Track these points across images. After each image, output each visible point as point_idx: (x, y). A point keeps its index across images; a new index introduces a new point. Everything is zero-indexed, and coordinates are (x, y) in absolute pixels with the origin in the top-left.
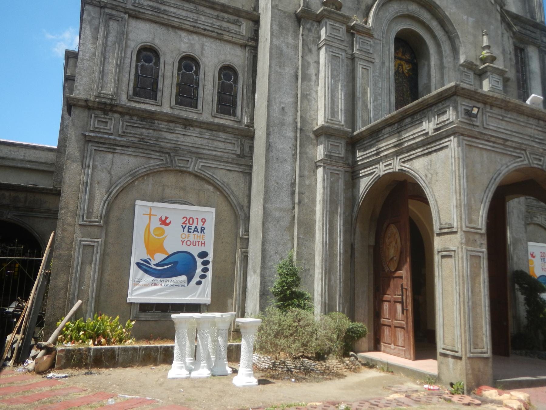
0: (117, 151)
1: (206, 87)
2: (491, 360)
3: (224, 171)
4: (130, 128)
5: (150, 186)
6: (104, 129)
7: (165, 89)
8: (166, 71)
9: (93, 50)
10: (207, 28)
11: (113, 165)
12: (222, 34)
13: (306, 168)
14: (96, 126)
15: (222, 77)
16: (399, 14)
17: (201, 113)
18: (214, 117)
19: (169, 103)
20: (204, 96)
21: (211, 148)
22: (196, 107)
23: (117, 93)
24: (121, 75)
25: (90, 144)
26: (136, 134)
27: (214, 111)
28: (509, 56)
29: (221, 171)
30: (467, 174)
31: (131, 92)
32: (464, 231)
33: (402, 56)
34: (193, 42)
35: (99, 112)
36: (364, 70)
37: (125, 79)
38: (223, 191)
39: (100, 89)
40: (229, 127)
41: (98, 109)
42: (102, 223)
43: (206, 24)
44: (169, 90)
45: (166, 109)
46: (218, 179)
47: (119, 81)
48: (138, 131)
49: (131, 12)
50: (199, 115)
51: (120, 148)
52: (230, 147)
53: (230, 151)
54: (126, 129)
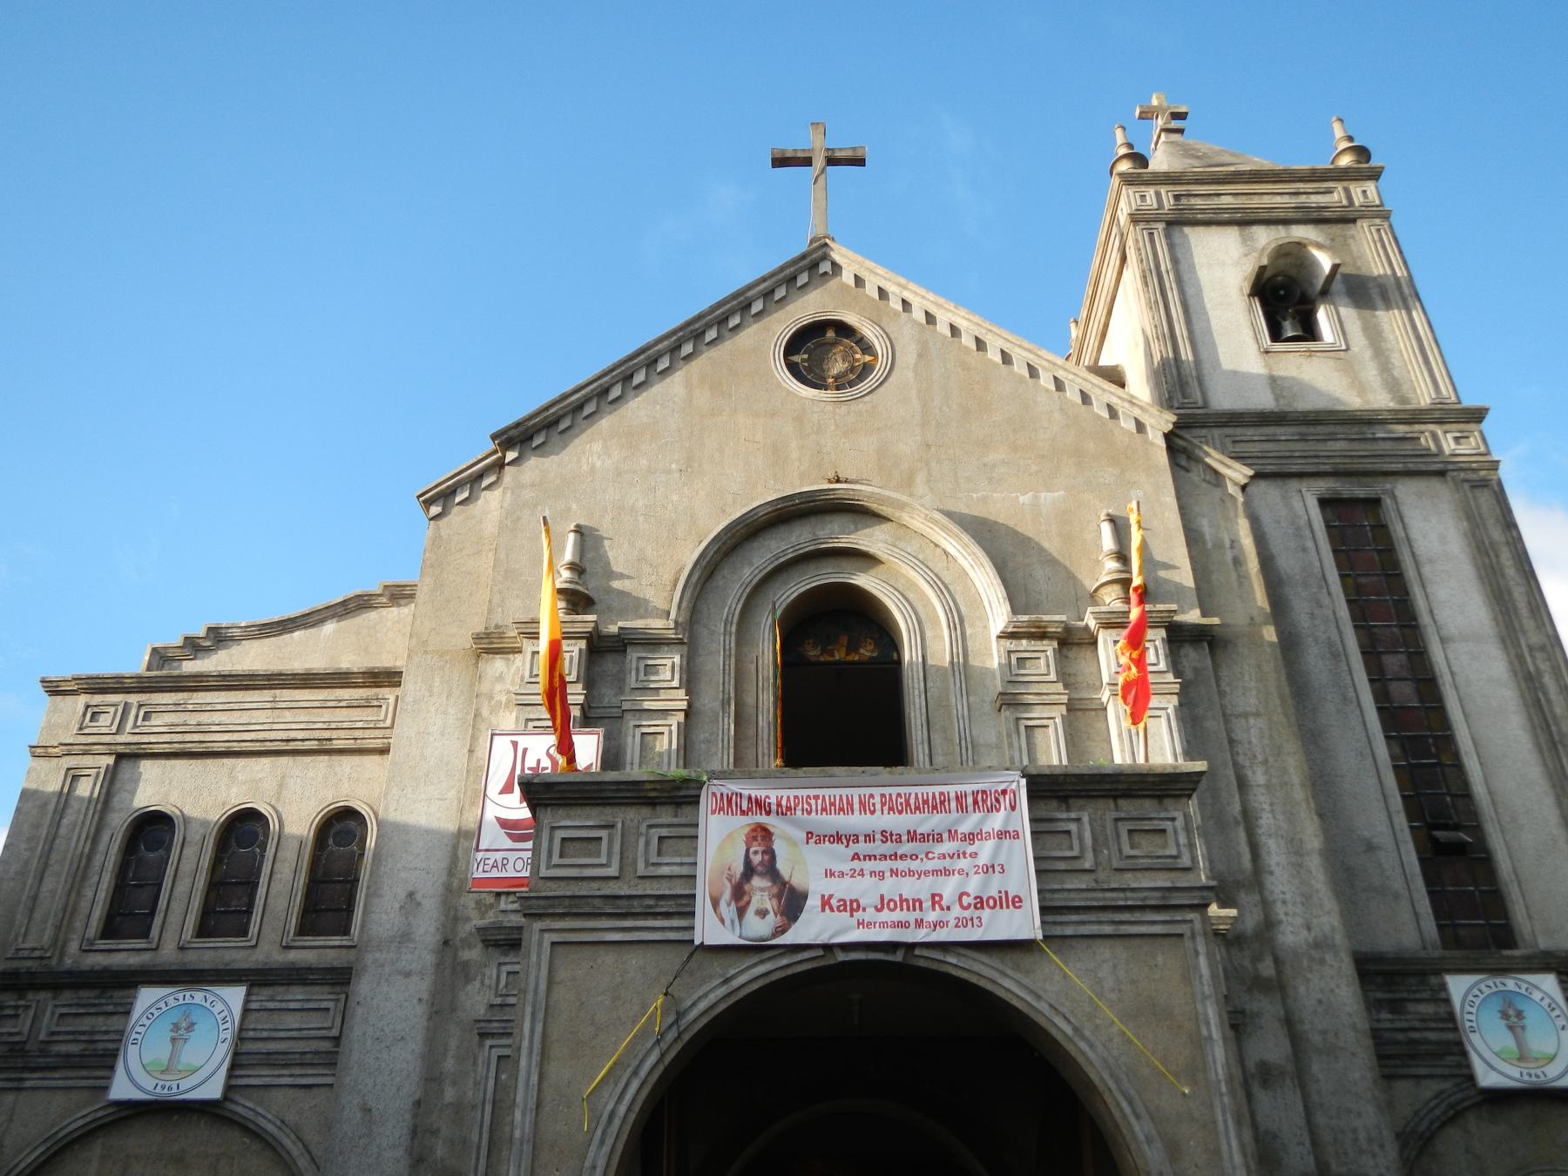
0: (28, 1084)
1: (277, 876)
3: (291, 1091)
4: (70, 1020)
6: (11, 1034)
7: (174, 905)
8: (183, 862)
9: (26, 855)
10: (293, 735)
11: (11, 1120)
12: (330, 740)
13: (451, 1054)
15: (331, 841)
16: (782, 560)
18: (288, 947)
19: (177, 938)
20: (269, 900)
21: (265, 1034)
22: (244, 932)
23: (59, 943)
24: (73, 895)
27: (289, 931)
28: (1229, 556)
29: (282, 1091)
30: (544, 1036)
31: (93, 930)
33: (848, 654)
36: (649, 738)
37: (84, 905)
39: (20, 939)
40: (310, 969)
43: (294, 726)
44: (184, 906)
45: (168, 954)
46: (270, 1117)
47: (69, 911)
48: (86, 1024)
49: (121, 749)
50: (249, 951)
51: (36, 1075)
52: (315, 1021)
53: (313, 1033)
54: (58, 1025)
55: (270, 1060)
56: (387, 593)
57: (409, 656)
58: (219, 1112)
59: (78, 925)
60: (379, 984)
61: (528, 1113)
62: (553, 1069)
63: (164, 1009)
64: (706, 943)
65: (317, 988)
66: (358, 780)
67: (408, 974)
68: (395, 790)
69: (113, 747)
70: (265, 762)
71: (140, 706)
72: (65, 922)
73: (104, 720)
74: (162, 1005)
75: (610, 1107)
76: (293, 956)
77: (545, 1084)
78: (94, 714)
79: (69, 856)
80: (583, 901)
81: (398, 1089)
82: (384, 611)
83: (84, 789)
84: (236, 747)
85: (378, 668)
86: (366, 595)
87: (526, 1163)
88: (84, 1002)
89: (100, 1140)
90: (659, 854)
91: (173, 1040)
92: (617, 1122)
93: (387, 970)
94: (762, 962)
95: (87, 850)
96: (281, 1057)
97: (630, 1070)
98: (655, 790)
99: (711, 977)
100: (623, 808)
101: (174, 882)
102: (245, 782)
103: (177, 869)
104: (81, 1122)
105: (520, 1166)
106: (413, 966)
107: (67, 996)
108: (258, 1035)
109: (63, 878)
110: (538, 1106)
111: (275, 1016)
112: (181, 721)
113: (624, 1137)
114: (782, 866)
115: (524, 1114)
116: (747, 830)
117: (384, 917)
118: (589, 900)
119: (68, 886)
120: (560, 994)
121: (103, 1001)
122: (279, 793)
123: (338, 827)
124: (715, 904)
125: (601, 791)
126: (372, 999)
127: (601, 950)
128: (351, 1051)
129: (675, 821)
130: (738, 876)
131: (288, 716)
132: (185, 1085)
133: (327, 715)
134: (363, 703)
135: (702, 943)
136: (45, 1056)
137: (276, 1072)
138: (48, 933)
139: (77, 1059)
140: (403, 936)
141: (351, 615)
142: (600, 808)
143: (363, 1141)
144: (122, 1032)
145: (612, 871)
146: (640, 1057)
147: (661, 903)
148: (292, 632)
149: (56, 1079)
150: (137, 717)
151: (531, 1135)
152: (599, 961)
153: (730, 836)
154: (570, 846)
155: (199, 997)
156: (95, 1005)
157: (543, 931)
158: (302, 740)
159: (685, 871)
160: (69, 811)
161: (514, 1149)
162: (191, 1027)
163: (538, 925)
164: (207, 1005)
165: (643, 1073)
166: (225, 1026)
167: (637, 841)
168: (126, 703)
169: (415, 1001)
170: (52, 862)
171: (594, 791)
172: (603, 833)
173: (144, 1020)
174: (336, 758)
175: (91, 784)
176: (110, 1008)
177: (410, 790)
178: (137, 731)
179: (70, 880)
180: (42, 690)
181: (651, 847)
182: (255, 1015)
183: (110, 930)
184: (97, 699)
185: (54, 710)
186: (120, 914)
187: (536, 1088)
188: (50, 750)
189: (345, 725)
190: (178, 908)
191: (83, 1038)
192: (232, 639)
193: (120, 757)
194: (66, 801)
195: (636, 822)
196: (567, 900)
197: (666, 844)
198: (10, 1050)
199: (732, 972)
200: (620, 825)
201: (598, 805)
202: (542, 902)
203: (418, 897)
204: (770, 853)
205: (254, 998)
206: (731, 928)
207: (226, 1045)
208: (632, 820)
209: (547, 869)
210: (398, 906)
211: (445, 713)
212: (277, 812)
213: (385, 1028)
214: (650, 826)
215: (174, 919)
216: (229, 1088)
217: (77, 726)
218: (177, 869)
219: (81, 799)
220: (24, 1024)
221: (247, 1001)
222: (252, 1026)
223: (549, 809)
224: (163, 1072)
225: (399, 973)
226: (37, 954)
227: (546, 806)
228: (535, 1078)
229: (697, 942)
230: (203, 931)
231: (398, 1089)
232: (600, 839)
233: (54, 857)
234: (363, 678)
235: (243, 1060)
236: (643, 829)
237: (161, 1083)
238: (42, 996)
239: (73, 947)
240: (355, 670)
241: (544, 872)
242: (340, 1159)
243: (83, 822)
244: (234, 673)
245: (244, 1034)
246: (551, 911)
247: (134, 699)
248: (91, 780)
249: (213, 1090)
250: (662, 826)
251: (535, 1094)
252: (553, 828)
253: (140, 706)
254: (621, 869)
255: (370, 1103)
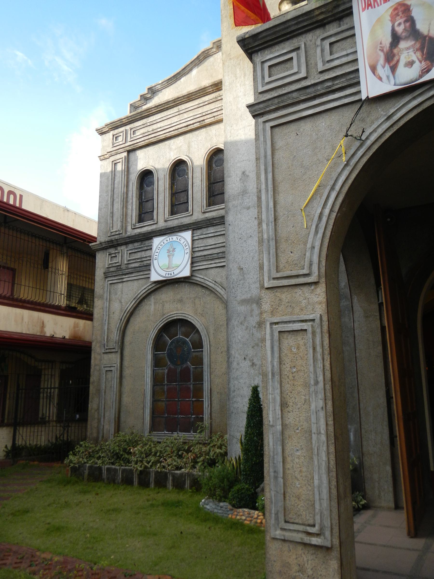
0: (125, 280)
2: (335, 554)
3: (217, 269)
4: (133, 255)
5: (153, 304)
6: (116, 263)
12: (204, 120)
14: (110, 263)
15: (214, 165)
17: (192, 214)
18: (204, 213)
21: (202, 248)
23: (124, 227)
25: (107, 280)
26: (138, 259)
27: (204, 206)
29: (212, 271)
31: (134, 222)
32: (267, 289)
34: (180, 145)
35: (112, 251)
37: (129, 212)
38: (216, 292)
40: (214, 219)
41: (111, 247)
42: (117, 348)
43: (189, 119)
44: (163, 205)
45: (161, 224)
46: (210, 280)
47: (125, 216)
48: (138, 255)
49: (128, 148)
51: (127, 276)
55: (206, 258)
56: (215, 46)
57: (223, 63)
58: (191, 281)
59: (129, 220)
60: (236, 215)
61: (270, 224)
62: (281, 198)
63: (163, 245)
64: (371, 96)
65: (219, 226)
66: (219, 135)
67: (248, 208)
68: (228, 128)
69: (125, 148)
70: (181, 138)
71: (131, 129)
72: (124, 219)
73: (120, 139)
74: (162, 243)
75: (319, 211)
76: (208, 215)
77: (278, 207)
78: (116, 137)
79: (120, 194)
80: (285, 97)
81: (253, 258)
82: (215, 56)
83: (119, 167)
84: (168, 135)
85: (217, 81)
86: (206, 50)
87: (273, 251)
88: (136, 247)
89: (153, 297)
90: (331, 54)
91: (169, 256)
92: (324, 219)
93: (239, 208)
94: (414, 98)
95: (125, 191)
96: (210, 256)
97: (329, 188)
98: (322, 13)
99: (377, 119)
100: (304, 36)
101: (158, 196)
102: (175, 149)
103: (158, 191)
104: (144, 291)
105: (269, 254)
106: (250, 204)
107: (131, 246)
108: (200, 249)
109: (120, 203)
110: (276, 219)
111: (205, 241)
112: (146, 131)
113: (330, 227)
114: (422, 26)
115: (267, 225)
116: (391, 10)
117: (234, 185)
118: (290, 95)
119: (122, 205)
120: (279, 154)
121: (142, 246)
122: (189, 150)
123: (216, 158)
124: (374, 69)
125: (287, 28)
126: (235, 222)
127: (302, 124)
128: (230, 245)
129: (339, 29)
130: (388, 45)
131: (186, 116)
132: (176, 272)
133: (200, 110)
134: (215, 100)
135: (368, 97)
136: (127, 269)
137: (209, 263)
138: (119, 224)
139: (138, 268)
140: (243, 192)
141: (203, 62)
142: (290, 41)
143: (242, 282)
144: (150, 256)
145: (303, 74)
146: (335, 178)
147: (336, 82)
148: (180, 79)
149: (133, 277)
150: (131, 134)
151: (274, 236)
152: (301, 130)
153: (379, 20)
154: (274, 69)
155: (175, 238)
156: (140, 248)
157: (265, 122)
158: (193, 124)
159: (350, 58)
160: (116, 178)
161: (265, 245)
162: (174, 250)
163: (261, 120)
164: (178, 241)
165: (338, 188)
166: (186, 247)
167: (316, 52)
168: (126, 130)
169: (253, 219)
170: (115, 198)
171: (283, 29)
172: (294, 55)
173: (157, 251)
174: (208, 128)
175: (121, 165)
176: (145, 248)
177: (235, 125)
178: (132, 139)
179: (122, 203)
180: (97, 134)
181: (326, 52)
182: (197, 241)
183: (141, 220)
184: (116, 131)
185: (103, 141)
186: (143, 213)
187: (273, 209)
188: (105, 156)
189: (209, 112)
190: (161, 206)
191: (138, 260)
192: (159, 91)
193: (129, 152)
194: (114, 174)
195: (313, 41)
196: (276, 99)
197: (336, 46)
198: (117, 269)
199: (392, 111)
200: (303, 46)
201: (288, 39)
202: (261, 106)
203: (247, 173)
204: (411, 21)
205: (195, 235)
206: (387, 81)
207: (188, 255)
208: (311, 41)
209: (262, 87)
210: (239, 179)
211: (245, 85)
212: (189, 158)
213: (243, 233)
214: (323, 39)
215: (161, 210)
216: (192, 271)
217: (112, 144)
218: (158, 191)
219: (119, 171)
220: (118, 260)
221: (193, 237)
222: (196, 246)
223: (259, 53)
224: (167, 269)
225: (244, 208)
226: (117, 233)
227: (257, 51)
228: (271, 204)
229: (364, 97)
230: (173, 212)
231: (253, 258)
232: (291, 59)
233: (115, 196)
234: (212, 88)
235: (195, 259)
236: (319, 42)
237: (167, 273)
238: (123, 247)
239: (129, 228)
240: (208, 85)
241: (261, 89)
242: (234, 290)
243: (122, 180)
244: (160, 104)
245: (194, 250)
246: (268, 109)
247: (128, 127)
248: (121, 163)
249: (186, 273)
250: (331, 36)
251: (273, 213)
252: (263, 63)
253: (131, 129)
254: (308, 72)
255: (242, 266)
